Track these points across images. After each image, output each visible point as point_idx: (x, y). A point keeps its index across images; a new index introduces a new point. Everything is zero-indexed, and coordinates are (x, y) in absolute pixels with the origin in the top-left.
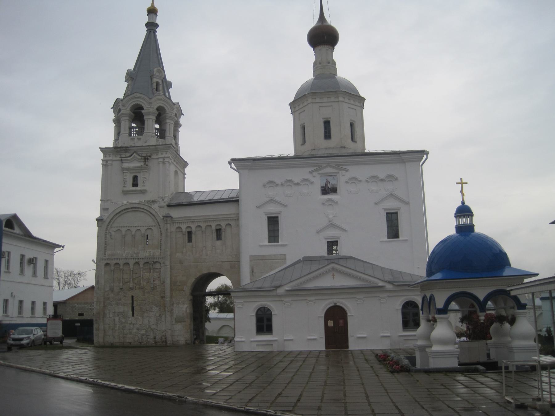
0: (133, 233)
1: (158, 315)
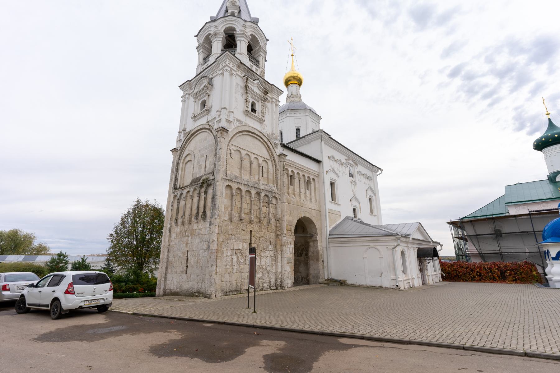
1: (273, 255)
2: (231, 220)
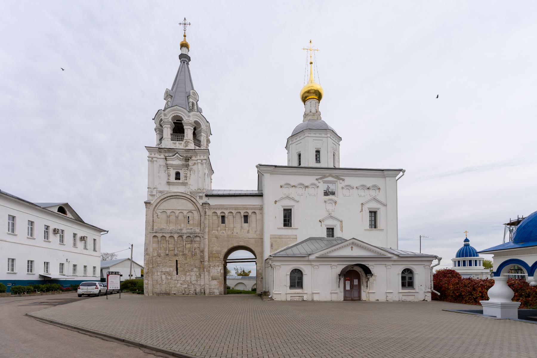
0: (177, 215)
1: (198, 274)
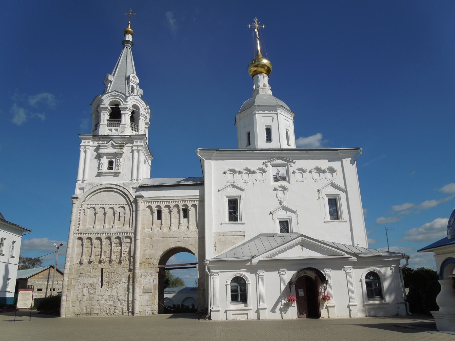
2: (81, 263)
